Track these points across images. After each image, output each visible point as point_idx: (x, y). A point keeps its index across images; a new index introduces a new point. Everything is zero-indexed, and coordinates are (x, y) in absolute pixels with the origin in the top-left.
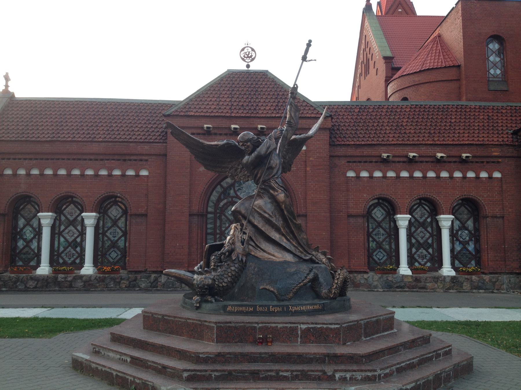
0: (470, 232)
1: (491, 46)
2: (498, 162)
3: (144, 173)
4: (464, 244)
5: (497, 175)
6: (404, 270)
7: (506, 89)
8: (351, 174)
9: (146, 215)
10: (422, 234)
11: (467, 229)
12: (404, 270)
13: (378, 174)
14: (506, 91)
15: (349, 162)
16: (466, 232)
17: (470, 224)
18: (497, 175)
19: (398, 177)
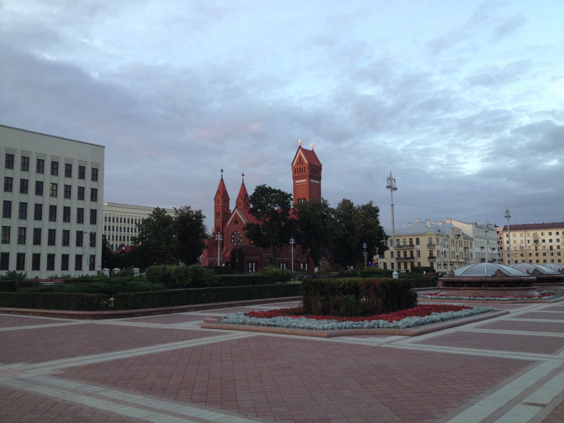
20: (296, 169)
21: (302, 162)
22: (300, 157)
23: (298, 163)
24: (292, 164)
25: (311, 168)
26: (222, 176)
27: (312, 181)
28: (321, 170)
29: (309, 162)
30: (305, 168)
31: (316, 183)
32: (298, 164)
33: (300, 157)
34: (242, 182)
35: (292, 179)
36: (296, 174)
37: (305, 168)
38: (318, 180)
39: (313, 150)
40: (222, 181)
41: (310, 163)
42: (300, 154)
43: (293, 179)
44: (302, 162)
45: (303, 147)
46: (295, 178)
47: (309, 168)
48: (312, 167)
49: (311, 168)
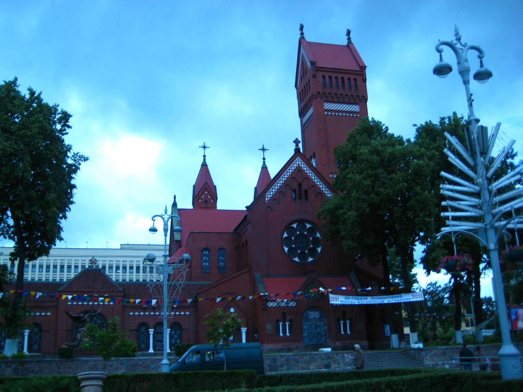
0: (178, 335)
1: (204, 253)
2: (188, 308)
3: (49, 314)
4: (176, 340)
5: (187, 313)
6: (151, 351)
7: (209, 272)
8: (131, 313)
9: (49, 331)
10: (159, 337)
11: (177, 334)
12: (151, 351)
13: (142, 313)
14: (210, 273)
15: (130, 309)
16: (177, 335)
17: (178, 332)
18: (187, 313)
19: (150, 314)
20: (300, 93)
21: (306, 70)
22: (303, 62)
23: (301, 77)
24: (296, 86)
25: (324, 76)
26: (204, 156)
27: (328, 106)
28: (365, 81)
29: (313, 63)
30: (309, 80)
31: (350, 112)
32: (302, 81)
33: (303, 62)
34: (262, 163)
35: (299, 117)
36: (302, 104)
37: (309, 80)
38: (356, 104)
39: (349, 46)
40: (204, 166)
41: (318, 65)
42: (303, 55)
43: (300, 118)
44: (306, 70)
45: (310, 38)
46: (302, 114)
47: (314, 76)
48: (327, 75)
49: (324, 76)
